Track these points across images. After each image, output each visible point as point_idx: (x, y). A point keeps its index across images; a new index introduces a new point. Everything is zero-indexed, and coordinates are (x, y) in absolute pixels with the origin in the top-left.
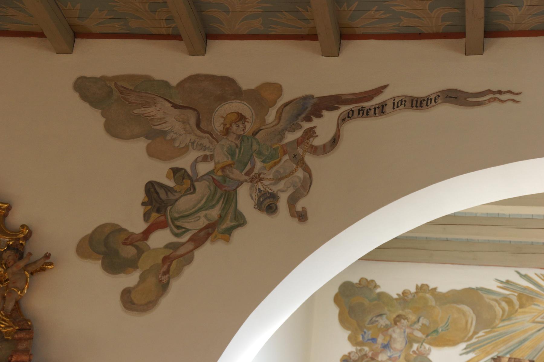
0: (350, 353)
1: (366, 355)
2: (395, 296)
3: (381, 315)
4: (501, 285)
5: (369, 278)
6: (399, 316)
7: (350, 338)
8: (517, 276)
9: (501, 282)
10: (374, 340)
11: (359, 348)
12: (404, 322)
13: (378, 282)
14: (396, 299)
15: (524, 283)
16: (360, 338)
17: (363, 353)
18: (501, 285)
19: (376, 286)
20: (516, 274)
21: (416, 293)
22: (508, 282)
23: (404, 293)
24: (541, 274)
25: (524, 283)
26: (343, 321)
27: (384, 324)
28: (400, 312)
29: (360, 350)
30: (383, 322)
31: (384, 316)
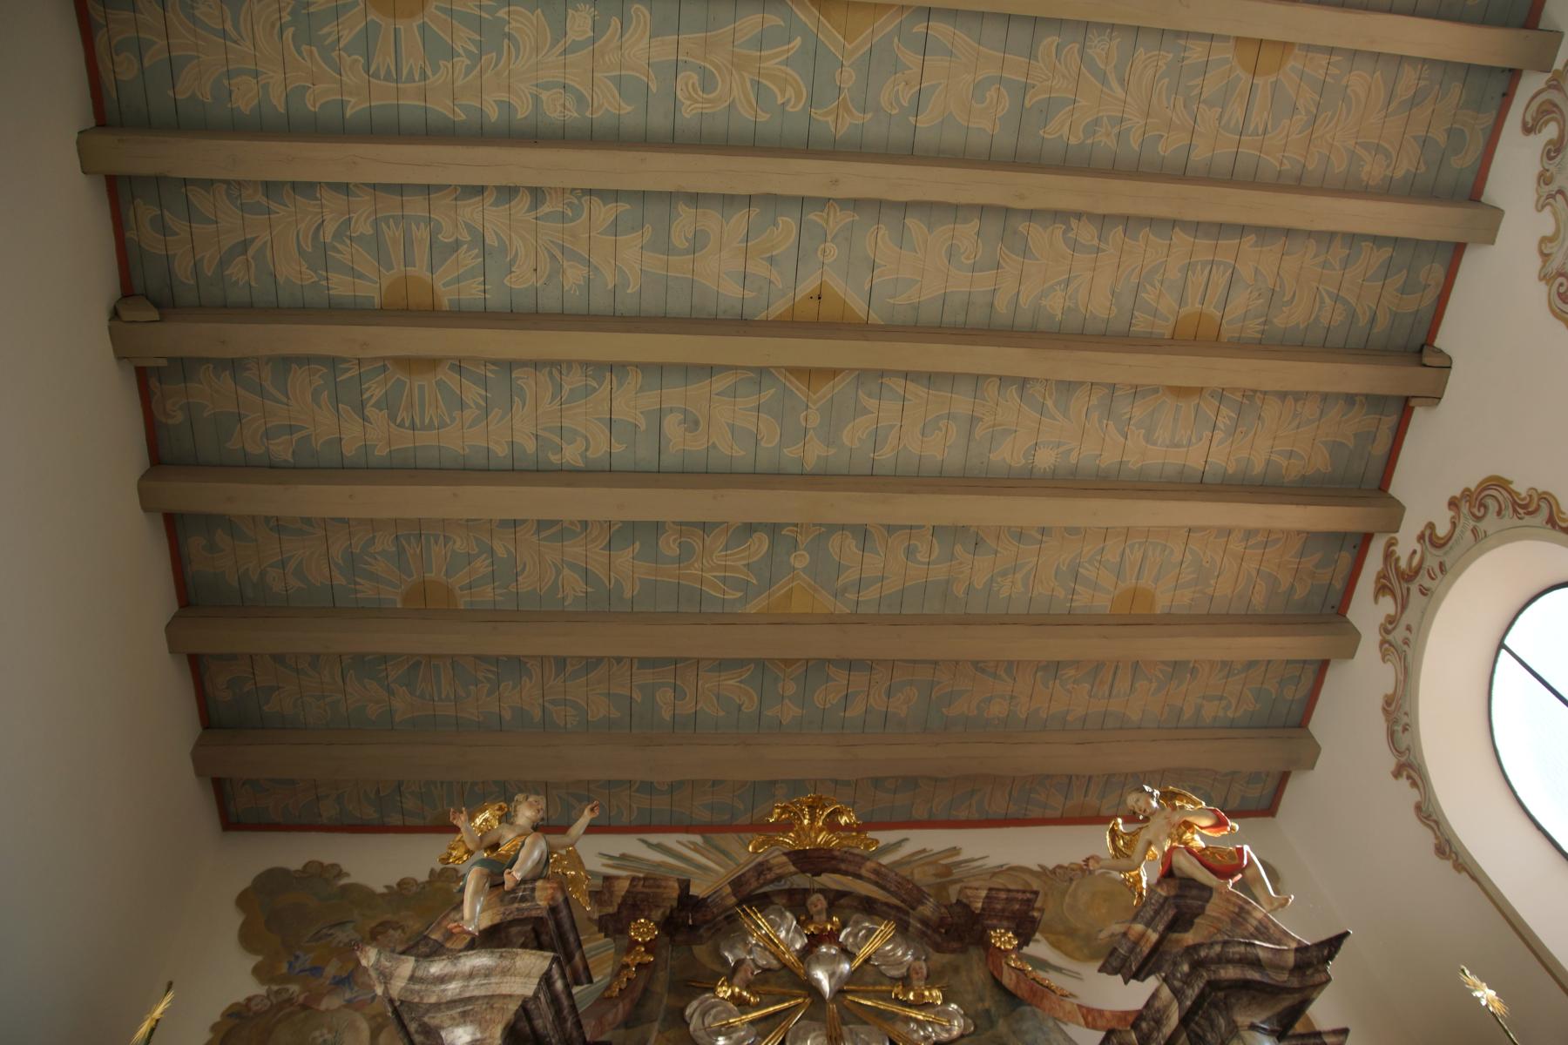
0: (249, 1000)
1: (290, 1001)
2: (380, 889)
3: (342, 924)
4: (610, 862)
5: (327, 860)
6: (382, 924)
7: (257, 971)
8: (644, 847)
9: (611, 857)
10: (316, 971)
11: (275, 988)
12: (397, 934)
13: (345, 868)
14: (382, 895)
15: (657, 857)
16: (284, 968)
17: (285, 996)
18: (610, 862)
19: (341, 874)
20: (641, 844)
21: (429, 882)
22: (623, 857)
23: (402, 884)
24: (689, 842)
25: (657, 857)
26: (248, 939)
27: (347, 940)
28: (388, 917)
29: (277, 992)
30: (342, 936)
31: (350, 926)
